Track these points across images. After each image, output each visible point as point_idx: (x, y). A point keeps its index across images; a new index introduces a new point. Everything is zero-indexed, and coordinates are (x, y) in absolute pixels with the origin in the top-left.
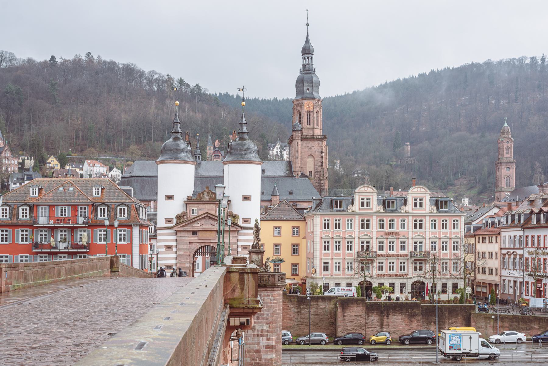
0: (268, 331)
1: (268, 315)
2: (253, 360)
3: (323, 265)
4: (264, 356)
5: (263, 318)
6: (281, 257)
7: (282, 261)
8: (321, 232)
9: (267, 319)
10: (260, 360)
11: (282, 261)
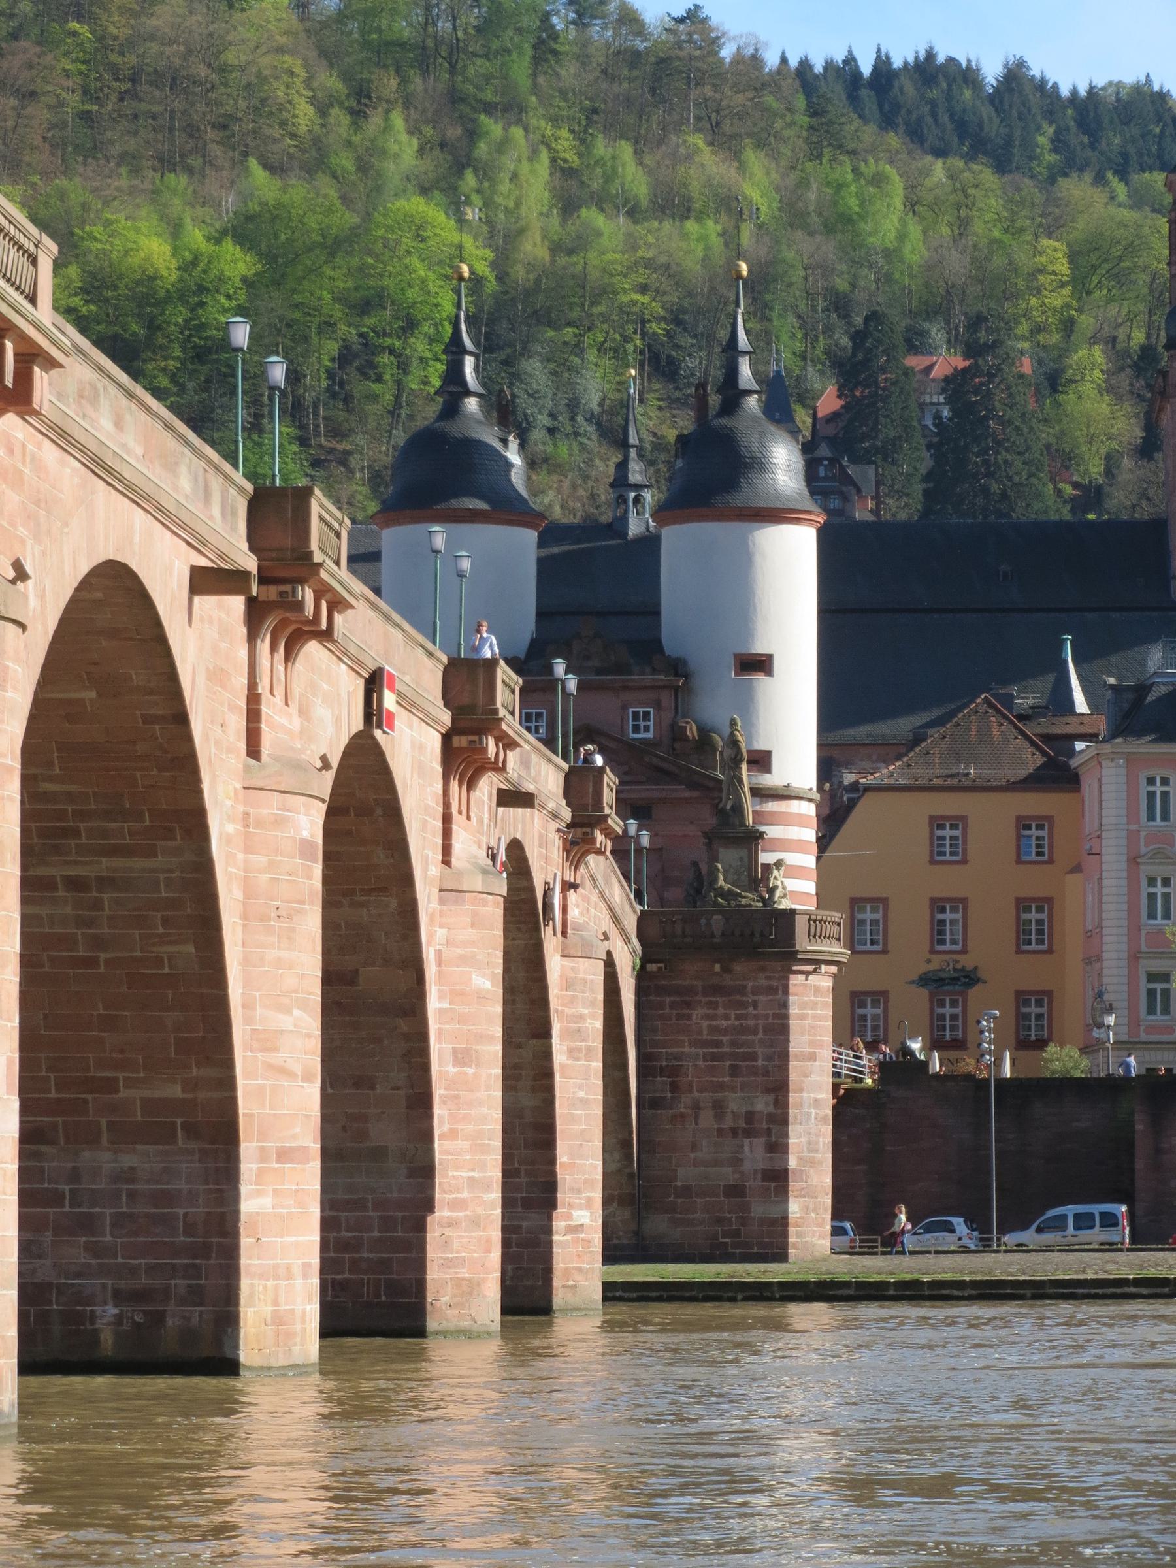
0: (772, 1118)
1: (769, 1058)
2: (720, 1221)
3: (1144, 986)
4: (758, 1210)
5: (754, 1072)
6: (967, 961)
7: (969, 978)
8: (1132, 837)
9: (767, 1074)
10: (744, 1221)
11: (969, 978)
